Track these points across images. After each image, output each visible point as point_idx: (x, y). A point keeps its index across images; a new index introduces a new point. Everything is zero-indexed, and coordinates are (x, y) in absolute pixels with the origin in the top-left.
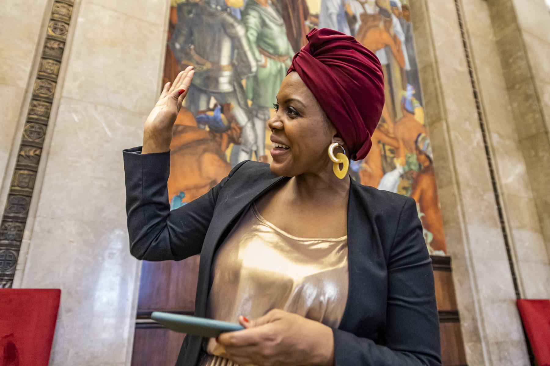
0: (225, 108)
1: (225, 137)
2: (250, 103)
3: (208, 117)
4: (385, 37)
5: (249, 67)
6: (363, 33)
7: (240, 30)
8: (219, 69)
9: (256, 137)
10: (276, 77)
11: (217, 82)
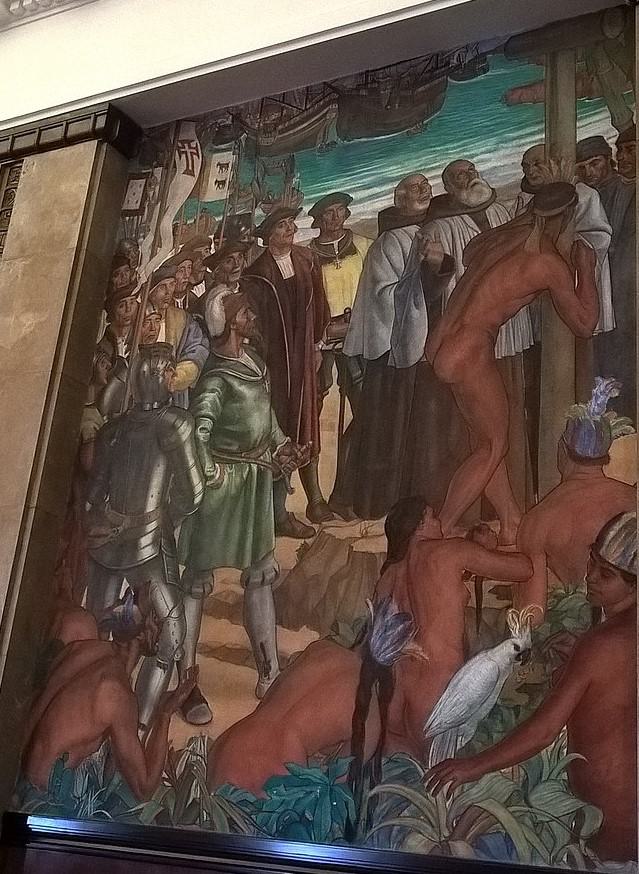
0: (141, 593)
1: (135, 644)
2: (182, 568)
3: (114, 617)
4: (543, 267)
5: (193, 496)
6: (465, 296)
7: (185, 430)
8: (142, 519)
9: (183, 634)
10: (236, 498)
11: (135, 547)
